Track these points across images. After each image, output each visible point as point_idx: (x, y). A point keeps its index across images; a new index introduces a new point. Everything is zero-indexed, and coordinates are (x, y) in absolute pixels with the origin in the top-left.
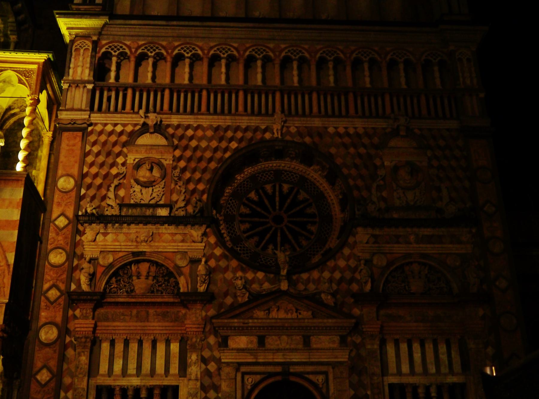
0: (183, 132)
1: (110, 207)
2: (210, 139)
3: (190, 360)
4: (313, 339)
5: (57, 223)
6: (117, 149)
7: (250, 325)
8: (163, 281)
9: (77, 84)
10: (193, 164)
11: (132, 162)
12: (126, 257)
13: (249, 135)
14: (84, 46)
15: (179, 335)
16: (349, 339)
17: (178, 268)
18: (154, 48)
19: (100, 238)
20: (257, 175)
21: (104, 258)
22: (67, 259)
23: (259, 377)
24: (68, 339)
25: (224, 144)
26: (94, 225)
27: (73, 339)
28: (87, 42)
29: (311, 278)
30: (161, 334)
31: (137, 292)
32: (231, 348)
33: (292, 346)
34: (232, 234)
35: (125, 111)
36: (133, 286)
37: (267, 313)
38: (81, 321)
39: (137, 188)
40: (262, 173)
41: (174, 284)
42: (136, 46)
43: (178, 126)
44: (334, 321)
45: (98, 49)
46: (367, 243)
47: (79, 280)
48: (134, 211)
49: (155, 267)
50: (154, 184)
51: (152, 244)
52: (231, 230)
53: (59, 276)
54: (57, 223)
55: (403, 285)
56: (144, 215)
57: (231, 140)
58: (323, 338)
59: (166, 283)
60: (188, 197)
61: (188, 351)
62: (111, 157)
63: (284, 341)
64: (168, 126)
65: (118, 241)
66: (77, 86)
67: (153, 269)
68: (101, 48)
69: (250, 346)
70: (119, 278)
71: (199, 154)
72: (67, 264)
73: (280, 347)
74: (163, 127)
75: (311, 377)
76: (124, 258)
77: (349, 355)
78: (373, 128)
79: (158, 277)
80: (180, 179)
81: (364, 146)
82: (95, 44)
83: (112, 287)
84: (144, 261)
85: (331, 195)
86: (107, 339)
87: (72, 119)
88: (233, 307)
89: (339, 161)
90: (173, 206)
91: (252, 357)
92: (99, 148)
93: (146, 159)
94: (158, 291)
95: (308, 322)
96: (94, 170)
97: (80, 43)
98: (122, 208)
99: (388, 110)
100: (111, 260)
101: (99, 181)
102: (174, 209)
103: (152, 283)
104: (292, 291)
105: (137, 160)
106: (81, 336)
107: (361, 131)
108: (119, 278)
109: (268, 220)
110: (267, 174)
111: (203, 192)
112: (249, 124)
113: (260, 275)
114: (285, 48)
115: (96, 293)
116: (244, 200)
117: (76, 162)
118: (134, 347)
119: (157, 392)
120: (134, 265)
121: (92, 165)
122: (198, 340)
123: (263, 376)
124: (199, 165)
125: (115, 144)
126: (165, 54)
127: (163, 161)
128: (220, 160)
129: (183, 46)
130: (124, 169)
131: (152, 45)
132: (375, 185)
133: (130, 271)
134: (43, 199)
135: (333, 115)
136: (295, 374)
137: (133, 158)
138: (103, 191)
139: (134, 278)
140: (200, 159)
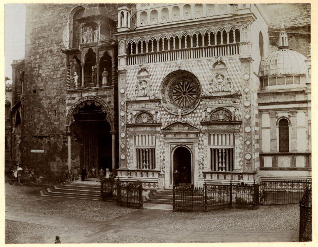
9: (122, 57)
10: (155, 81)
16: (199, 135)
23: (176, 146)
24: (127, 136)
25: (164, 73)
46: (205, 104)
64: (148, 68)
67: (147, 115)
68: (127, 42)
74: (146, 69)
75: (188, 146)
82: (125, 41)
86: (137, 135)
104: (181, 122)
113: (175, 116)
118: (144, 137)
119: (150, 150)
140: (157, 79)
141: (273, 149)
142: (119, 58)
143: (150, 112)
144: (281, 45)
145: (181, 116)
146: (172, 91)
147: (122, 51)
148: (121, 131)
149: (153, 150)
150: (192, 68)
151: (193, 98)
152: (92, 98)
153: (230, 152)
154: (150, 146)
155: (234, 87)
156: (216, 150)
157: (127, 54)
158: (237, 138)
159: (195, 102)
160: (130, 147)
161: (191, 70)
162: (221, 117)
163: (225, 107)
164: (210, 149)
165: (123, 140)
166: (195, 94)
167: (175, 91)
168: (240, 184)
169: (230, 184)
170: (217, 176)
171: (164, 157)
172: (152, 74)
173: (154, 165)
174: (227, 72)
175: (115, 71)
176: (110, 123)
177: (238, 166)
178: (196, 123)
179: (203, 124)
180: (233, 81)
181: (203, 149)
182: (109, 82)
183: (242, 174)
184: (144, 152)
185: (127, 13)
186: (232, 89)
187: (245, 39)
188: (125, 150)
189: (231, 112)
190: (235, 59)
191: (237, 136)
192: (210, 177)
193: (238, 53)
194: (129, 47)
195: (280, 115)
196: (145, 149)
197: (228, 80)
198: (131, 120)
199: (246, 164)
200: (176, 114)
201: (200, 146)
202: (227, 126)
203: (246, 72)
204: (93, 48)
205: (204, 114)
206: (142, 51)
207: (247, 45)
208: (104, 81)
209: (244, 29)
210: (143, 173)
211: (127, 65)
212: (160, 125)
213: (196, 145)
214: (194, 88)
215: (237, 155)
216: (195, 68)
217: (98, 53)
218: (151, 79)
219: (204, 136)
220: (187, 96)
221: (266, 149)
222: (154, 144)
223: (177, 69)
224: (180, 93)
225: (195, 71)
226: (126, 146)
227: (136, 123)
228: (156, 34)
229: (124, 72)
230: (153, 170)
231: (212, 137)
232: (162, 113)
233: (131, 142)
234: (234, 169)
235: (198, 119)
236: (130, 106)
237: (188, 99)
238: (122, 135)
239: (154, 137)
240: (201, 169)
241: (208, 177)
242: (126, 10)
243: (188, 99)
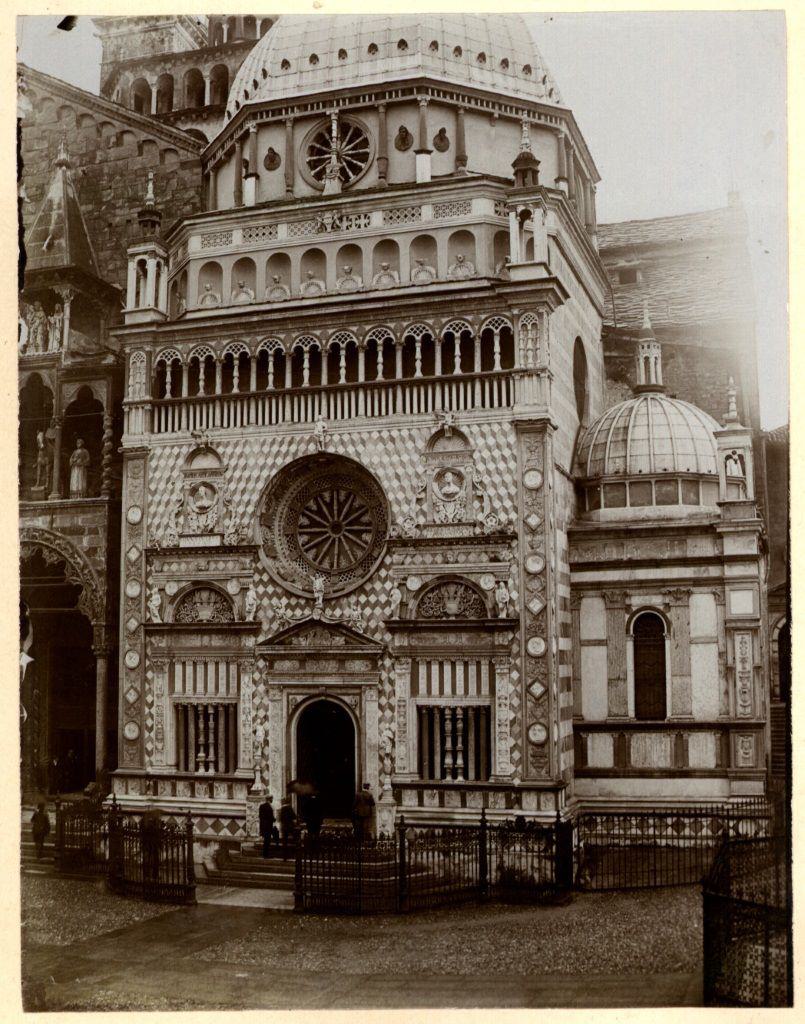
10: (242, 485)
13: (293, 448)
16: (380, 663)
24: (148, 663)
25: (270, 461)
46: (403, 564)
64: (219, 444)
66: (137, 408)
67: (213, 596)
68: (156, 358)
74: (214, 447)
82: (149, 354)
84: (205, 589)
89: (380, 472)
100: (175, 590)
102: (225, 537)
104: (324, 620)
113: (303, 602)
118: (200, 669)
119: (221, 709)
123: (304, 697)
126: (215, 357)
132: (414, 500)
136: (332, 696)
140: (248, 479)
141: (615, 710)
142: (126, 409)
144: (642, 381)
145: (324, 600)
146: (297, 519)
147: (137, 387)
148: (127, 647)
149: (230, 711)
150: (360, 448)
151: (362, 544)
152: (34, 537)
153: (481, 718)
154: (222, 696)
155: (494, 511)
156: (436, 711)
157: (152, 395)
158: (501, 674)
159: (370, 555)
160: (155, 698)
161: (358, 454)
162: (452, 607)
163: (465, 576)
164: (415, 709)
165: (133, 675)
167: (304, 521)
168: (512, 822)
169: (480, 821)
170: (437, 795)
171: (267, 733)
172: (233, 463)
173: (232, 760)
175: (113, 451)
176: (90, 618)
177: (504, 764)
178: (373, 624)
179: (393, 627)
180: (491, 491)
181: (392, 708)
182: (92, 485)
183: (520, 790)
184: (201, 717)
185: (158, 265)
186: (488, 517)
187: (530, 360)
188: (138, 711)
189: (483, 591)
190: (500, 424)
191: (502, 667)
192: (415, 802)
193: (508, 404)
194: (161, 375)
195: (637, 601)
196: (206, 707)
197: (474, 487)
198: (158, 610)
199: (531, 759)
200: (308, 595)
201: (383, 698)
203: (532, 464)
204: (44, 374)
205: (397, 595)
206: (202, 390)
207: (535, 378)
208: (77, 480)
209: (529, 327)
210: (197, 785)
211: (152, 431)
212: (254, 629)
213: (372, 696)
214: (367, 511)
215: (504, 729)
216: (370, 447)
217: (61, 392)
218: (230, 480)
219: (397, 666)
220: (344, 535)
221: (595, 708)
222: (233, 691)
223: (312, 449)
224: (319, 525)
225: (371, 457)
226: (141, 697)
228: (248, 334)
229: (143, 453)
230: (230, 775)
231: (422, 670)
232: (261, 589)
233: (159, 682)
234: (493, 773)
235: (378, 611)
236: (157, 564)
237: (347, 548)
238: (131, 660)
239: (233, 668)
240: (386, 774)
241: (410, 800)
242: (153, 254)
243: (347, 548)
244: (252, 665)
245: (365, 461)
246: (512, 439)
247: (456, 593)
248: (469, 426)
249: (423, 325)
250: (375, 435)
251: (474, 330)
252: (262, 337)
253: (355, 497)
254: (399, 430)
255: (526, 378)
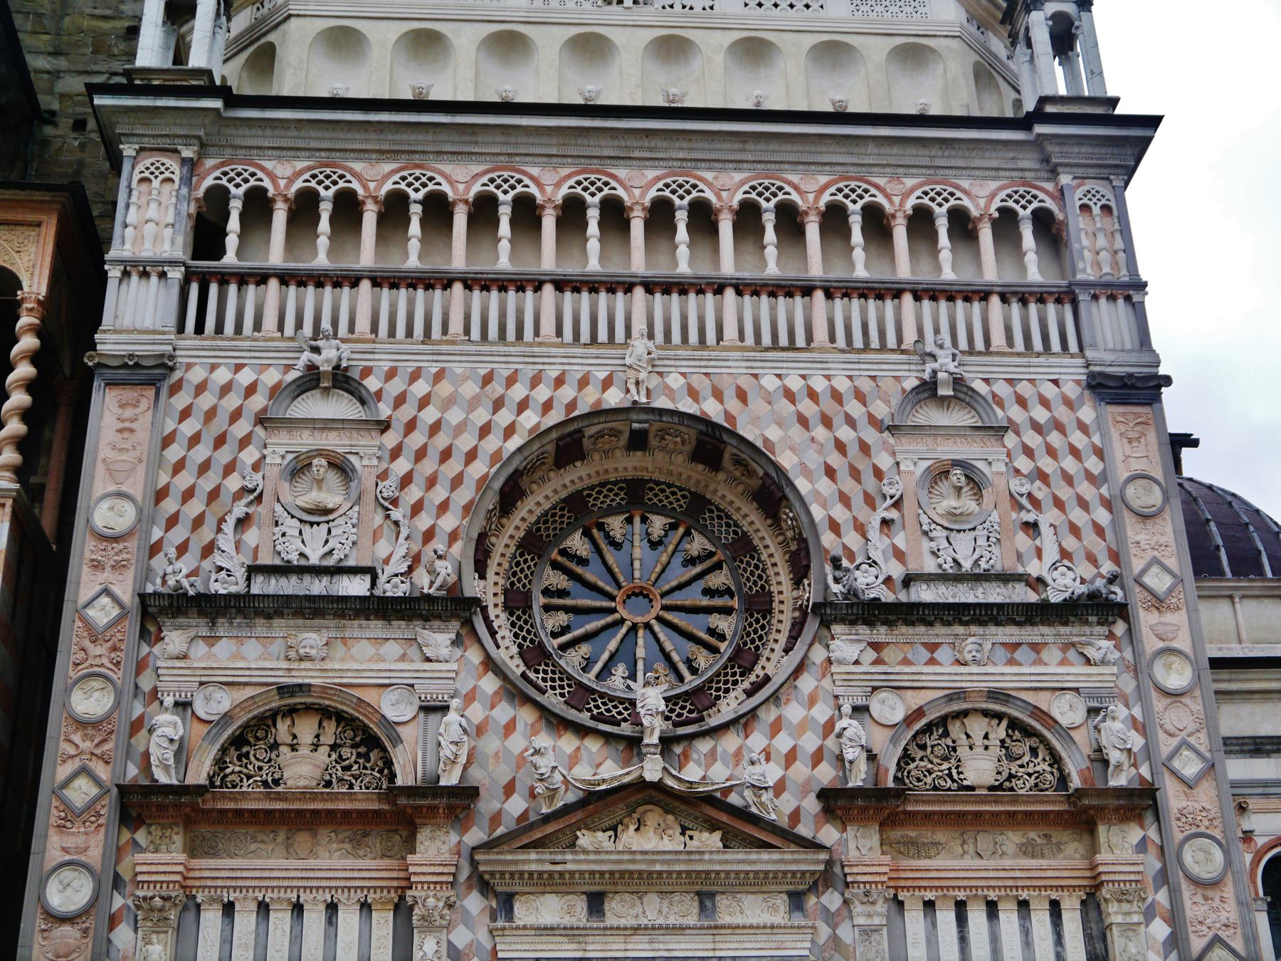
0: (404, 387)
1: (224, 572)
2: (473, 404)
3: (421, 953)
4: (722, 902)
5: (91, 612)
6: (242, 428)
7: (570, 867)
8: (354, 757)
9: (142, 269)
10: (428, 466)
11: (279, 461)
12: (263, 697)
13: (567, 393)
14: (162, 173)
15: (392, 891)
16: (812, 901)
17: (390, 725)
18: (335, 177)
19: (200, 649)
20: (585, 493)
21: (207, 699)
22: (117, 704)
24: (118, 902)
26: (182, 620)
27: (130, 902)
28: (168, 162)
29: (719, 750)
30: (349, 888)
31: (289, 783)
32: (521, 923)
33: (672, 920)
34: (524, 639)
35: (261, 334)
36: (280, 768)
37: (610, 837)
38: (149, 857)
39: (291, 526)
40: (598, 489)
41: (380, 763)
42: (288, 173)
43: (391, 374)
44: (776, 856)
45: (194, 179)
46: (857, 662)
47: (147, 755)
48: (283, 581)
49: (333, 724)
50: (331, 517)
51: (327, 665)
52: (521, 629)
53: (97, 745)
54: (91, 612)
55: (945, 766)
56: (308, 593)
57: (523, 406)
58: (748, 900)
59: (361, 761)
60: (415, 548)
61: (415, 931)
62: (225, 447)
63: (653, 910)
65: (244, 658)
67: (331, 727)
69: (568, 921)
70: (245, 750)
71: (442, 441)
72: (115, 715)
73: (643, 921)
74: (355, 374)
76: (257, 700)
77: (813, 941)
78: (873, 378)
79: (340, 746)
80: (395, 502)
81: (851, 422)
82: (191, 166)
83: (228, 771)
84: (308, 708)
85: (768, 541)
86: (212, 900)
87: (130, 355)
88: (525, 824)
89: (786, 460)
90: (379, 571)
91: (574, 946)
92: (198, 427)
93: (311, 454)
94: (340, 780)
95: (710, 861)
96: (184, 480)
97: (152, 164)
98: (253, 576)
99: (910, 336)
100: (225, 706)
101: (195, 507)
102: (382, 579)
103: (327, 760)
104: (670, 782)
105: (290, 457)
106: (150, 894)
107: (842, 385)
108: (245, 750)
109: (613, 604)
110: (610, 490)
111: (453, 537)
112: (567, 367)
113: (593, 745)
114: (658, 179)
115: (188, 786)
116: (554, 555)
117: (140, 461)
118: (280, 920)
120: (283, 717)
121: (179, 466)
122: (441, 904)
124: (442, 468)
125: (236, 415)
126: (361, 192)
127: (353, 459)
128: (496, 457)
129: (405, 173)
130: (255, 480)
131: (328, 171)
132: (878, 521)
133: (273, 730)
134: (54, 547)
135: (775, 346)
137: (281, 451)
138: (207, 533)
139: (284, 749)
140: (446, 455)
142: (114, 273)
143: (368, 696)
145: (661, 739)
150: (733, 405)
155: (1065, 554)
161: (729, 417)
166: (727, 611)
174: (1004, 457)
178: (787, 803)
186: (1054, 567)
190: (1055, 382)
191: (1125, 907)
202: (1032, 835)
209: (1096, 210)
211: (181, 329)
214: (718, 566)
216: (757, 405)
219: (858, 908)
220: (658, 619)
227: (212, 784)
236: (175, 639)
239: (383, 923)
244: (450, 906)
245: (750, 437)
246: (1087, 413)
247: (986, 737)
248: (986, 381)
249: (864, 186)
250: (770, 382)
251: (977, 206)
252: (481, 168)
253: (687, 533)
254: (828, 377)
255: (1103, 301)
